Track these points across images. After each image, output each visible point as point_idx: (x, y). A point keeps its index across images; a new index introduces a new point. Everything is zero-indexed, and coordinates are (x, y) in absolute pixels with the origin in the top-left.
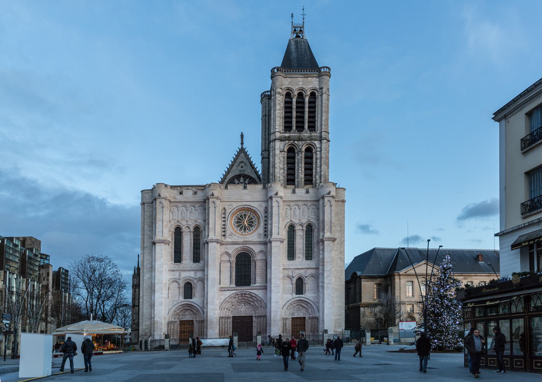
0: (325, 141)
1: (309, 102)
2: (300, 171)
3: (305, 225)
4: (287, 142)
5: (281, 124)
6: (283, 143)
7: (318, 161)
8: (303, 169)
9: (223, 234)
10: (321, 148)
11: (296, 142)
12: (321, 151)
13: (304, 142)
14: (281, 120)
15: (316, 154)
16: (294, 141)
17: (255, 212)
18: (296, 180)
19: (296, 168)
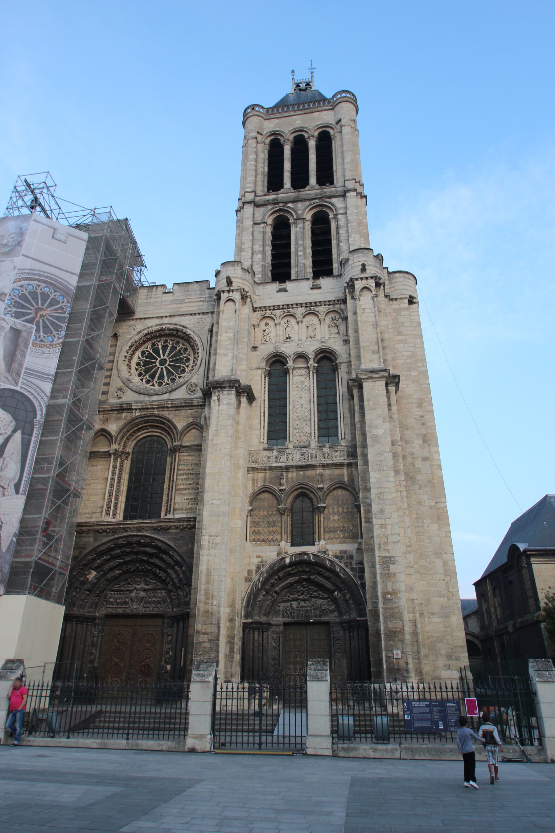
0: (354, 193)
1: (318, 148)
2: (300, 254)
3: (312, 356)
4: (270, 207)
5: (260, 183)
6: (262, 209)
7: (342, 231)
8: (309, 251)
9: (105, 389)
10: (346, 208)
11: (290, 205)
12: (346, 213)
13: (307, 203)
14: (260, 178)
15: (337, 220)
16: (286, 203)
17: (187, 339)
18: (293, 272)
19: (293, 249)
